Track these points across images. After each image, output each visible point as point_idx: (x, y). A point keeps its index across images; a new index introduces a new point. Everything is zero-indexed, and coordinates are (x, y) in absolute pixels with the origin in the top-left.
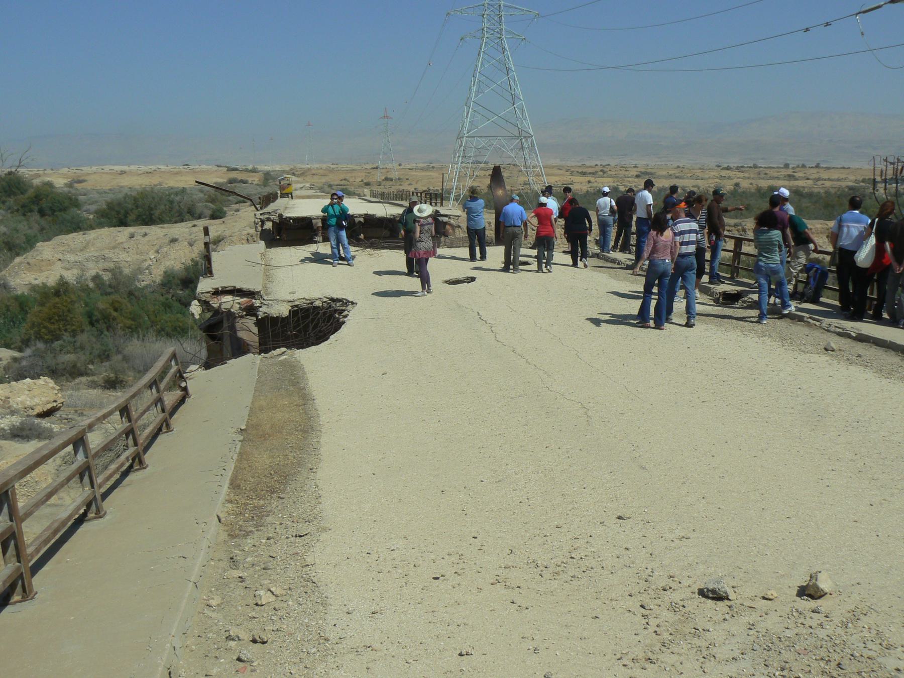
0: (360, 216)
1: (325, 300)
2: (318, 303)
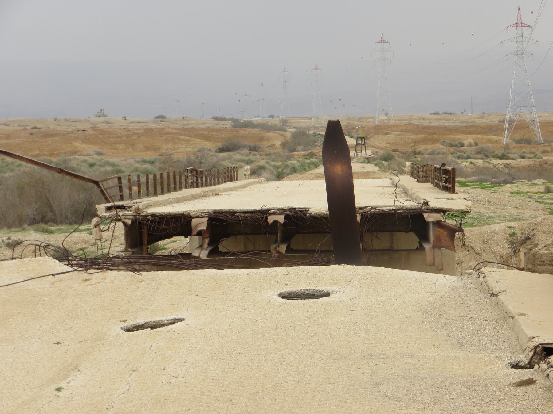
0: (281, 211)
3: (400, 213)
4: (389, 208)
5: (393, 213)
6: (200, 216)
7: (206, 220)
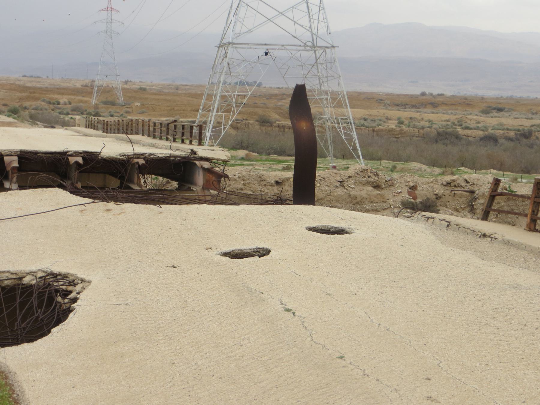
0: (77, 154)
1: (40, 274)
2: (27, 280)
3: (173, 160)
4: (165, 155)
5: (167, 159)
6: (11, 154)
7: (16, 158)
